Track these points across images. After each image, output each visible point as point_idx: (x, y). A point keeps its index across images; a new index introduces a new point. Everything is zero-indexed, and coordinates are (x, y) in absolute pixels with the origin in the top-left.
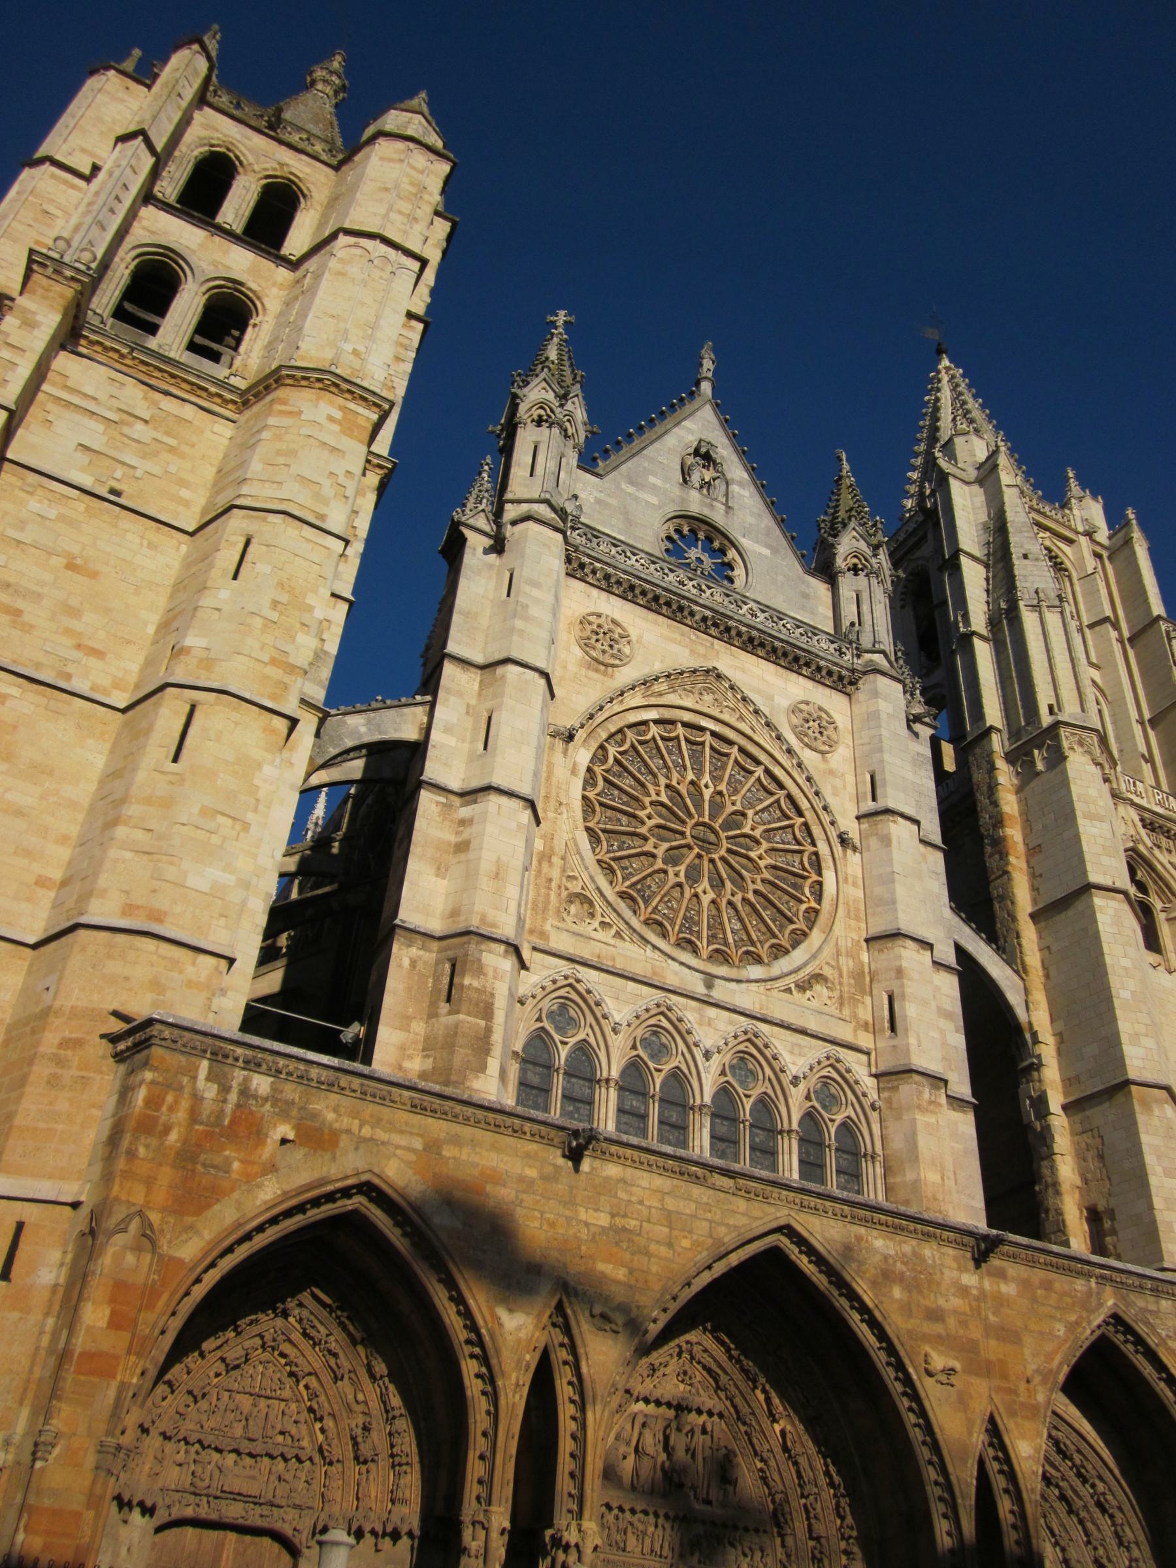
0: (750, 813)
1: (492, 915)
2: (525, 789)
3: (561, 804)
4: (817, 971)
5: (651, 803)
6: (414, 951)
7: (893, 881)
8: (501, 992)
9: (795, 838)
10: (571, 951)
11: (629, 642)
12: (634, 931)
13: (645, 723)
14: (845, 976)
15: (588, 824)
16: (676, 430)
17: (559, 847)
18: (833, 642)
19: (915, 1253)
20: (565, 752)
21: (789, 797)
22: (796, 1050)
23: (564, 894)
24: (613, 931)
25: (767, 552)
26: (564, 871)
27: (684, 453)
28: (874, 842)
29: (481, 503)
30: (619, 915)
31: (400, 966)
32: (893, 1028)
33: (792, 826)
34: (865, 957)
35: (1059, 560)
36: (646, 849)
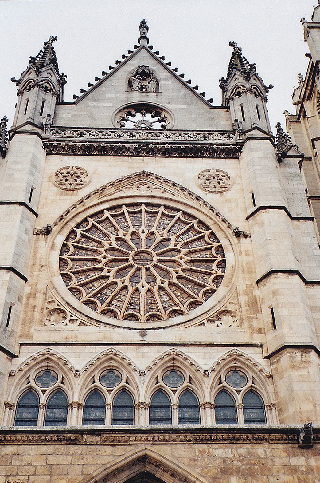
0: (173, 238)
2: (8, 264)
3: (42, 266)
4: (222, 309)
12: (91, 318)
13: (102, 212)
14: (243, 306)
18: (223, 135)
19: (249, 453)
20: (46, 241)
22: (207, 356)
23: (46, 311)
24: (79, 322)
25: (185, 106)
30: (81, 313)
33: (203, 237)
34: (257, 292)
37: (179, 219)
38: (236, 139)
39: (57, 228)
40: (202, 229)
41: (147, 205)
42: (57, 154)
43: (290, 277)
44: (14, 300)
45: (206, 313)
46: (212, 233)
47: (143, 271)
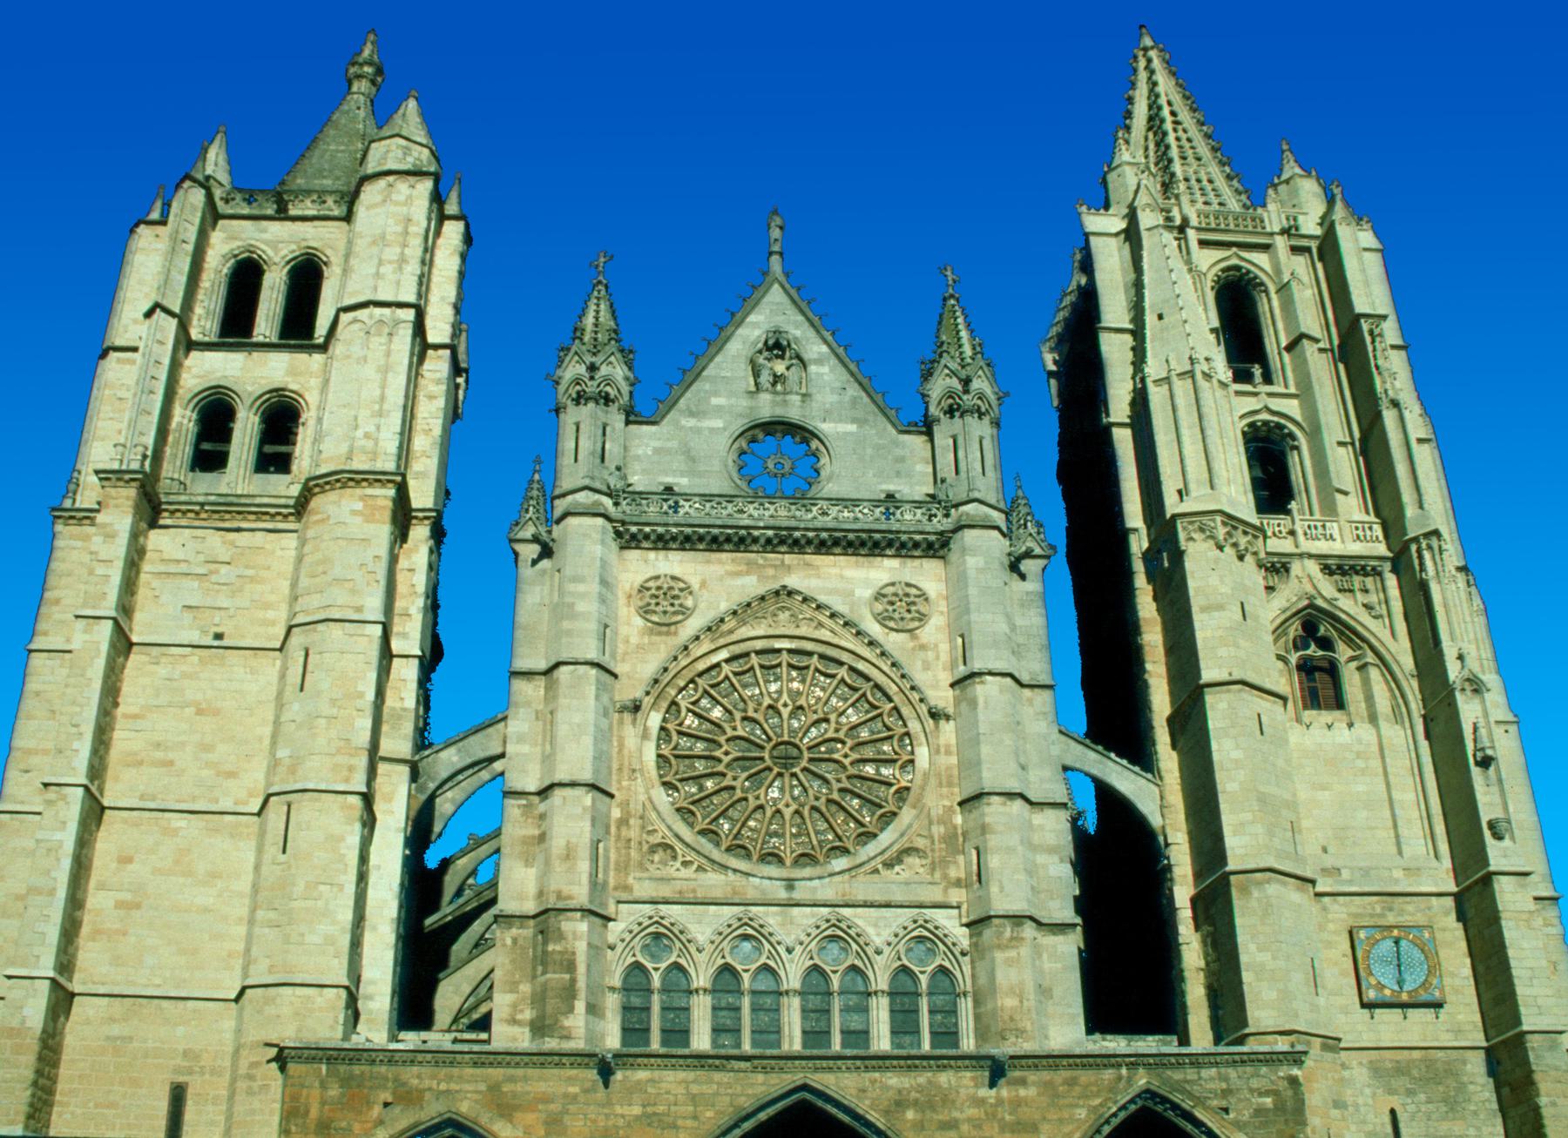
0: (833, 717)
1: (566, 890)
2: (586, 776)
3: (634, 771)
4: (906, 846)
5: (728, 740)
6: (514, 931)
7: (978, 743)
8: (581, 948)
9: (885, 725)
10: (654, 894)
11: (691, 593)
15: (665, 779)
16: (740, 331)
17: (635, 807)
21: (877, 686)
23: (645, 847)
24: (695, 866)
25: (853, 428)
26: (643, 827)
27: (750, 355)
28: (964, 706)
29: (527, 511)
31: (504, 945)
32: (980, 881)
33: (880, 715)
34: (958, 819)
35: (1251, 275)
36: (723, 785)
37: (843, 680)
38: (941, 523)
39: (647, 701)
40: (879, 700)
41: (790, 651)
42: (638, 548)
43: (1009, 803)
44: (601, 832)
45: (882, 853)
46: (896, 708)
47: (787, 779)
